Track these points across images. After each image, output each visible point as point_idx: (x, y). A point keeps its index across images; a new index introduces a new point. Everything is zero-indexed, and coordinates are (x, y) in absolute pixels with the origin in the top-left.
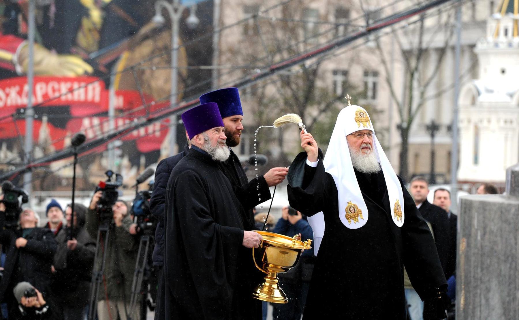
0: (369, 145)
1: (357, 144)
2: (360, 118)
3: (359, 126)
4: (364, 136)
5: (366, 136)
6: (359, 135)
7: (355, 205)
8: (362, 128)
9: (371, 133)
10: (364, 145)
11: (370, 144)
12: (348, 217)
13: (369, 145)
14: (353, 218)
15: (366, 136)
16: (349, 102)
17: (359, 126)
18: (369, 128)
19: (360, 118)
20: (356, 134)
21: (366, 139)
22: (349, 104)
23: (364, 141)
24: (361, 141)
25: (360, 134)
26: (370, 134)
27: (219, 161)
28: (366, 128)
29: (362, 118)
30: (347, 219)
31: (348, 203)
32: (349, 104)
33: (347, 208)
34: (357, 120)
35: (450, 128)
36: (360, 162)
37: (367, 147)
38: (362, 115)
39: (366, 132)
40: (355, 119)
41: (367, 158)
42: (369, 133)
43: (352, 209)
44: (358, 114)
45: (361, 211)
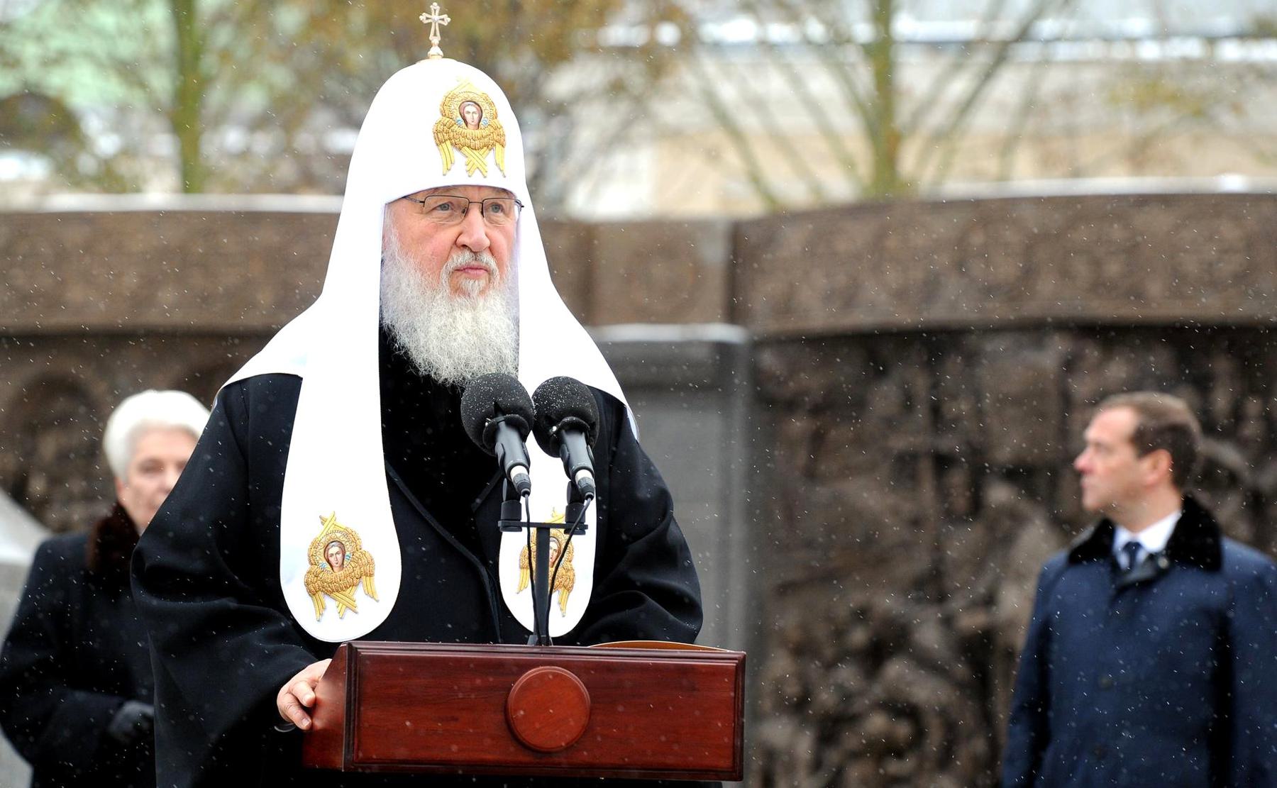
0: (487, 258)
1: (428, 249)
2: (460, 129)
3: (449, 166)
4: (465, 211)
5: (475, 213)
6: (444, 207)
7: (348, 533)
8: (458, 176)
9: (506, 203)
10: (463, 258)
11: (491, 249)
12: (316, 589)
13: (487, 258)
14: (331, 590)
15: (475, 213)
16: (435, 40)
17: (449, 166)
18: (495, 180)
19: (460, 129)
20: (432, 202)
21: (477, 227)
22: (435, 50)
23: (463, 239)
24: (448, 235)
25: (448, 202)
26: (497, 207)
27: (229, 213)
28: (477, 180)
29: (470, 131)
30: (312, 593)
31: (323, 521)
32: (435, 50)
33: (315, 545)
34: (444, 135)
35: (491, 249)
36: (433, 330)
37: (472, 269)
38: (472, 118)
39: (477, 196)
40: (436, 132)
41: (468, 315)
42: (496, 202)
43: (334, 550)
44: (455, 107)
45: (371, 562)
